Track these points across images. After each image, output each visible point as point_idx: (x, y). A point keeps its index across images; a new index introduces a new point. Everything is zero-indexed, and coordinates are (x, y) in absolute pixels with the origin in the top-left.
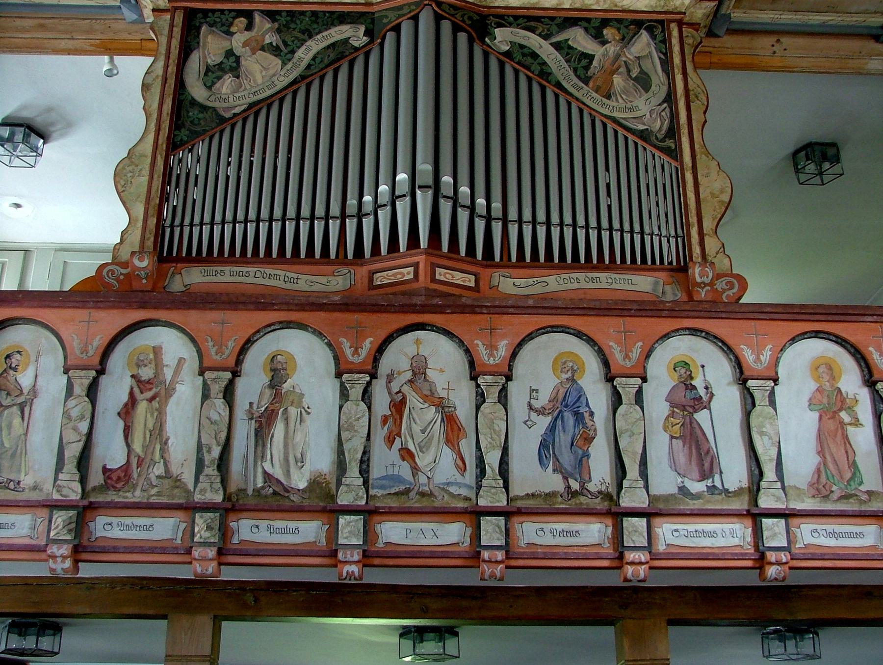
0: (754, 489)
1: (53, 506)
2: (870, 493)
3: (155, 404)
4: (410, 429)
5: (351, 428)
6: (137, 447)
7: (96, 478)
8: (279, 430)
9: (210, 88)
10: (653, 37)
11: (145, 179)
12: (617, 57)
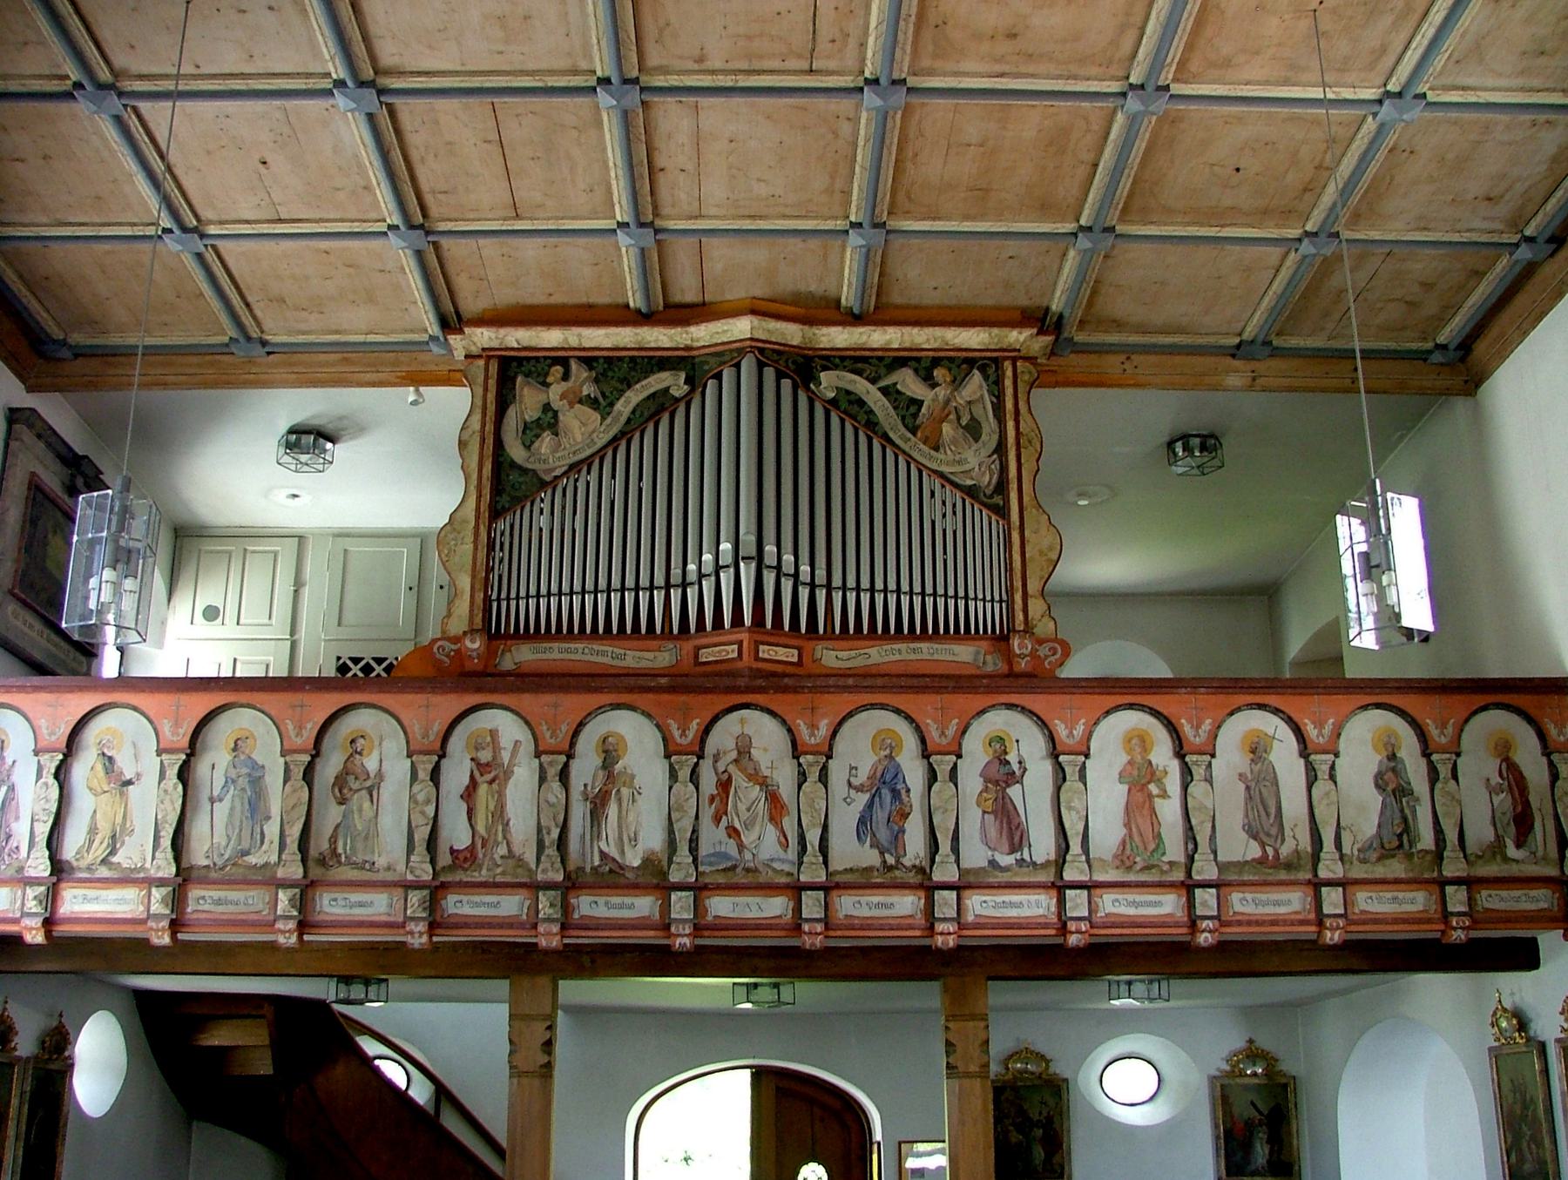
0: (1060, 862)
1: (408, 886)
2: (1171, 863)
3: (495, 786)
4: (735, 806)
5: (680, 808)
6: (481, 829)
7: (444, 859)
8: (612, 810)
9: (528, 447)
10: (986, 378)
11: (469, 547)
12: (947, 402)
